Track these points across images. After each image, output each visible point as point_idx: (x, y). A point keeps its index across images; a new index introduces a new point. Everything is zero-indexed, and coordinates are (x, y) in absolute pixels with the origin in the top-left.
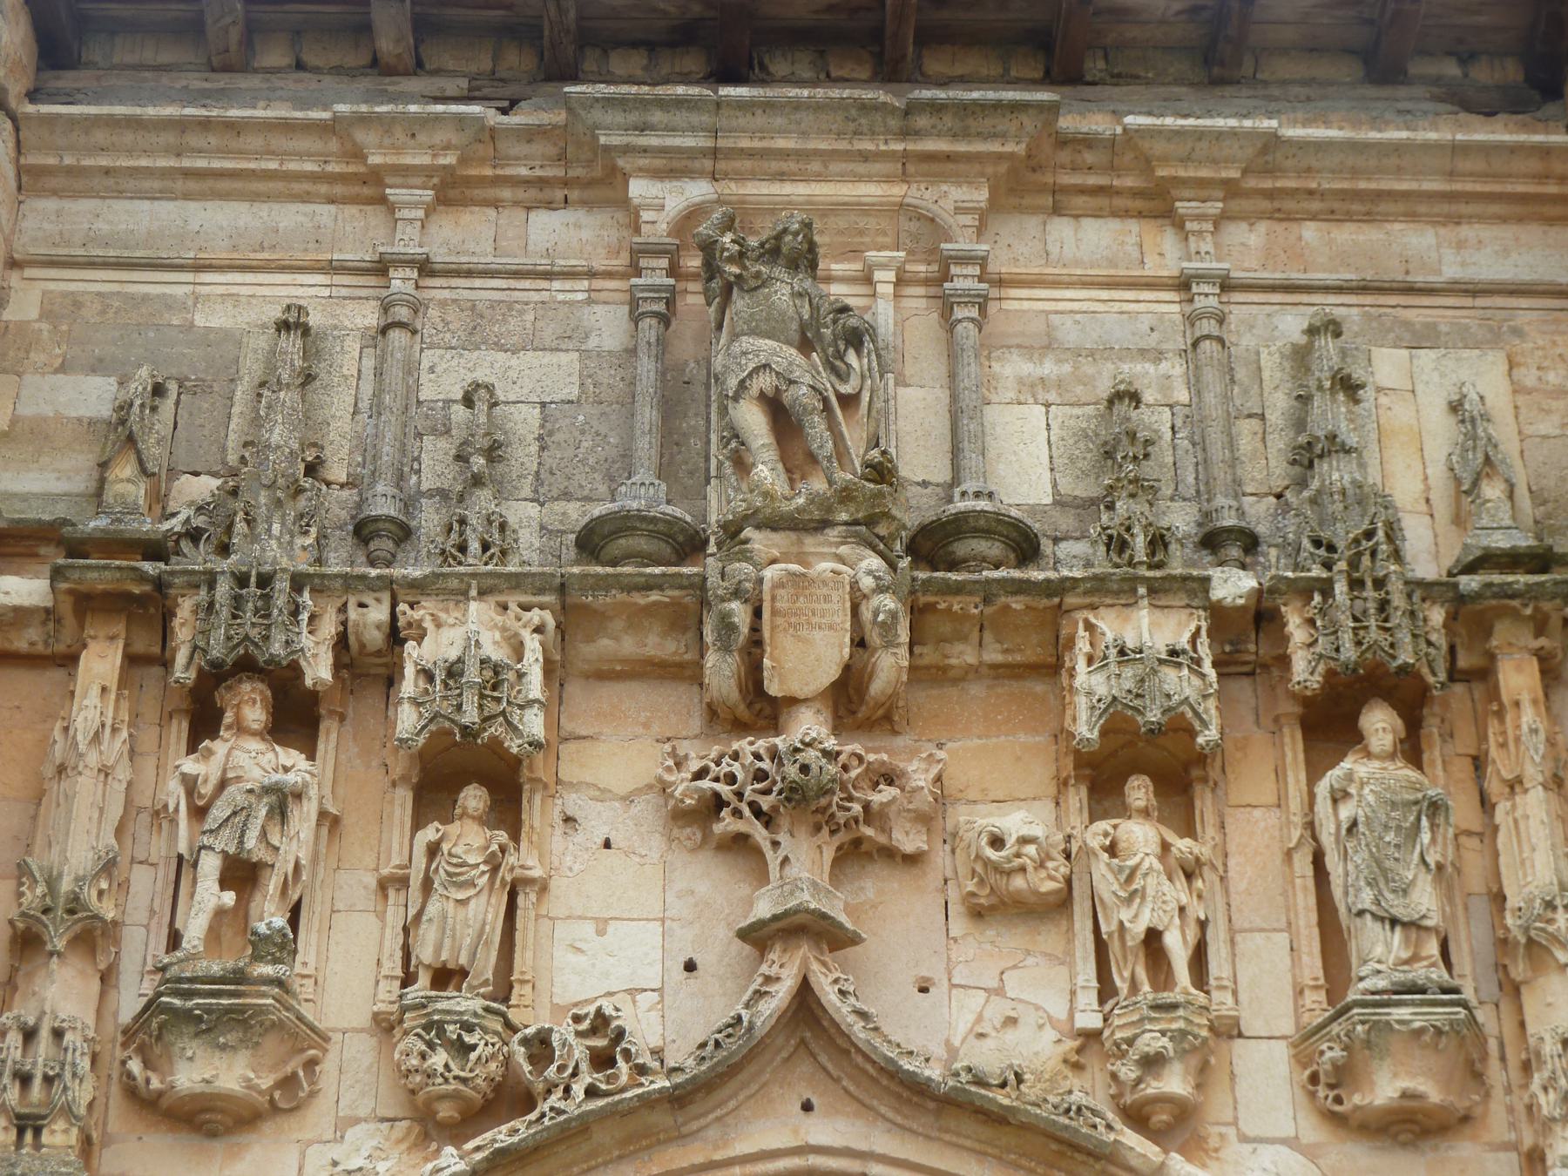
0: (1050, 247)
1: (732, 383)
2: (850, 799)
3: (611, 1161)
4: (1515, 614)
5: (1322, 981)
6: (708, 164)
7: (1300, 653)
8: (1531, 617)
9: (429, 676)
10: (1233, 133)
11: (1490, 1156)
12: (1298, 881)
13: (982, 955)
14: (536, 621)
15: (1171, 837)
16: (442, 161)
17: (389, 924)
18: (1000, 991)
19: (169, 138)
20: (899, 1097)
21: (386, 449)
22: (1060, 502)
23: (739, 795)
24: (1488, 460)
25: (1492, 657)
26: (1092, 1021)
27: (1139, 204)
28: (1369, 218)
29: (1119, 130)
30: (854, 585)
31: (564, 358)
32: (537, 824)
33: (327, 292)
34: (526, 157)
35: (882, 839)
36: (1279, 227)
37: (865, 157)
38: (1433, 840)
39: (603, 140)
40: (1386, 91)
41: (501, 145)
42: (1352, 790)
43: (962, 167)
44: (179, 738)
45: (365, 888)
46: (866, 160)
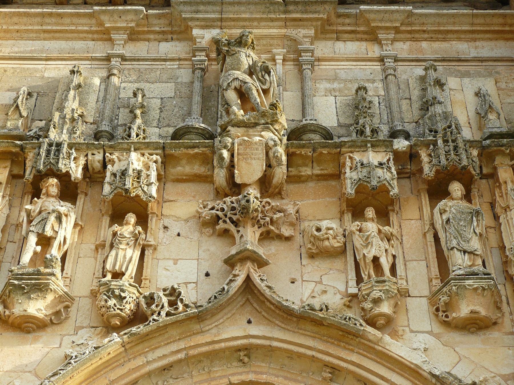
0: (336, 50)
1: (225, 84)
2: (266, 216)
3: (176, 341)
4: (503, 153)
5: (439, 276)
6: (219, 23)
7: (426, 165)
8: (509, 154)
9: (115, 175)
10: (397, 11)
11: (506, 336)
12: (429, 243)
13: (314, 269)
14: (155, 159)
15: (381, 228)
16: (130, 25)
17: (98, 260)
18: (321, 282)
19: (39, 19)
20: (283, 317)
21: (107, 111)
22: (340, 125)
23: (226, 216)
24: (490, 106)
25: (495, 168)
26: (353, 290)
27: (366, 36)
28: (444, 40)
29: (358, 11)
30: (267, 144)
31: (169, 85)
32: (153, 227)
33: (90, 66)
34: (158, 24)
35: (277, 231)
36: (414, 43)
37: (272, 20)
38: (478, 225)
39: (183, 16)
40: (449, 4)
41: (150, 20)
42: (447, 209)
43: (305, 23)
44: (27, 201)
45: (91, 249)
46: (273, 21)
